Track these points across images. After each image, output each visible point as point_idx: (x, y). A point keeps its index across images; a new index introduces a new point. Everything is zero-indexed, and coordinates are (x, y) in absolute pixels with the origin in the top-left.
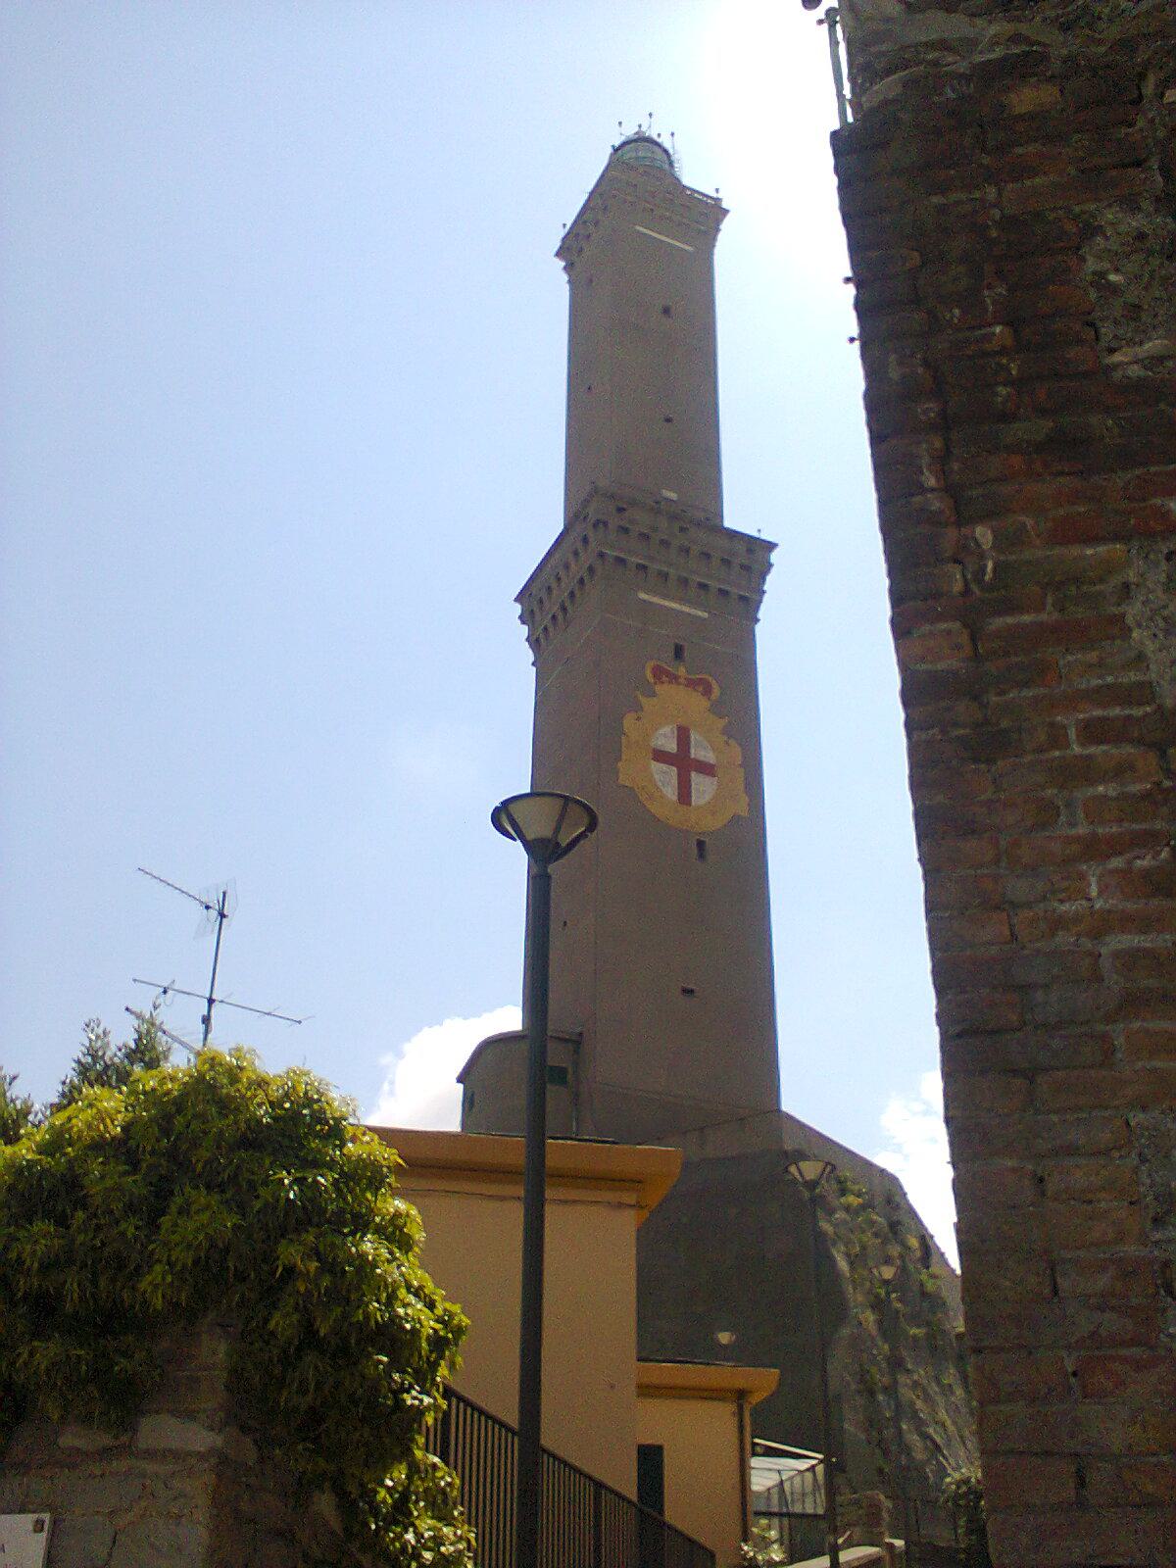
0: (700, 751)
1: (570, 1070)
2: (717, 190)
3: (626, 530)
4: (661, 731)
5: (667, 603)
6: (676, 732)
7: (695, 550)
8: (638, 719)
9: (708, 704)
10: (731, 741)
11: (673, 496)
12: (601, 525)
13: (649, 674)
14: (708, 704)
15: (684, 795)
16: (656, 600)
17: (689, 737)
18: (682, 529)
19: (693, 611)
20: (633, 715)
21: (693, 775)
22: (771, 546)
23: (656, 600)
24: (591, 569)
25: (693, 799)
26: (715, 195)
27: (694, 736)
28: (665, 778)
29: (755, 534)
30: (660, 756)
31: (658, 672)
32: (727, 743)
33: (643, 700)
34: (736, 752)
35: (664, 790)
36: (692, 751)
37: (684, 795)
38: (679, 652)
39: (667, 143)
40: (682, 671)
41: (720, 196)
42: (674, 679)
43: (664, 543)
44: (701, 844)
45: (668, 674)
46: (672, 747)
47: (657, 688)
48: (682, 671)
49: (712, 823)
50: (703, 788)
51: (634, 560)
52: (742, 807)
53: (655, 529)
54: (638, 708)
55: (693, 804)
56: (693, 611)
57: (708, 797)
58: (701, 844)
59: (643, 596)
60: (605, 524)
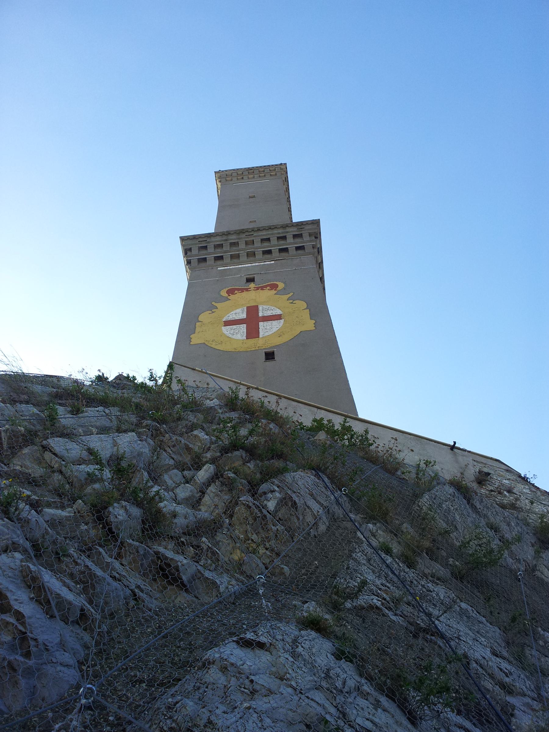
6: (245, 310)
12: (189, 253)
13: (224, 293)
21: (261, 324)
23: (231, 267)
34: (302, 305)
35: (234, 337)
40: (252, 285)
45: (238, 289)
53: (226, 240)
55: (260, 336)
57: (275, 330)
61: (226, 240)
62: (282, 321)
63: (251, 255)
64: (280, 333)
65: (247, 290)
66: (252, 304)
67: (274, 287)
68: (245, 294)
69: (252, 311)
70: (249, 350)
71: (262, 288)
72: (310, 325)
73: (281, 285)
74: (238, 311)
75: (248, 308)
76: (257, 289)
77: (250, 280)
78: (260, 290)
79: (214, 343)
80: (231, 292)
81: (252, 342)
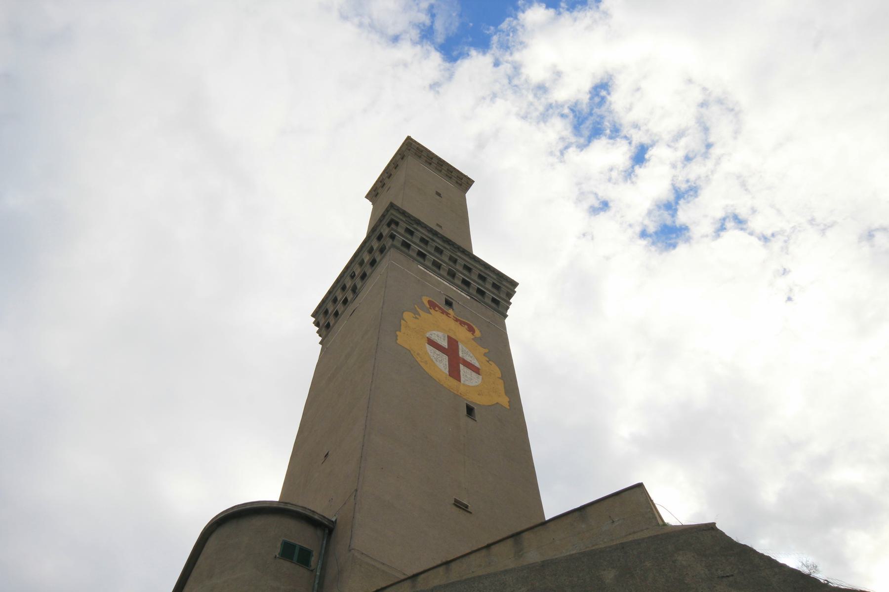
1: (315, 554)
9: (472, 337)
12: (393, 226)
14: (469, 335)
15: (454, 373)
17: (458, 346)
21: (461, 366)
25: (462, 379)
35: (437, 363)
37: (454, 373)
40: (450, 311)
44: (470, 411)
45: (440, 308)
46: (445, 344)
52: (504, 401)
60: (397, 224)
62: (480, 377)
63: (452, 274)
65: (447, 314)
66: (454, 337)
67: (471, 330)
68: (444, 316)
69: (453, 343)
71: (462, 323)
72: (504, 401)
73: (478, 333)
74: (440, 334)
75: (449, 337)
76: (457, 320)
77: (449, 303)
78: (458, 323)
80: (432, 305)
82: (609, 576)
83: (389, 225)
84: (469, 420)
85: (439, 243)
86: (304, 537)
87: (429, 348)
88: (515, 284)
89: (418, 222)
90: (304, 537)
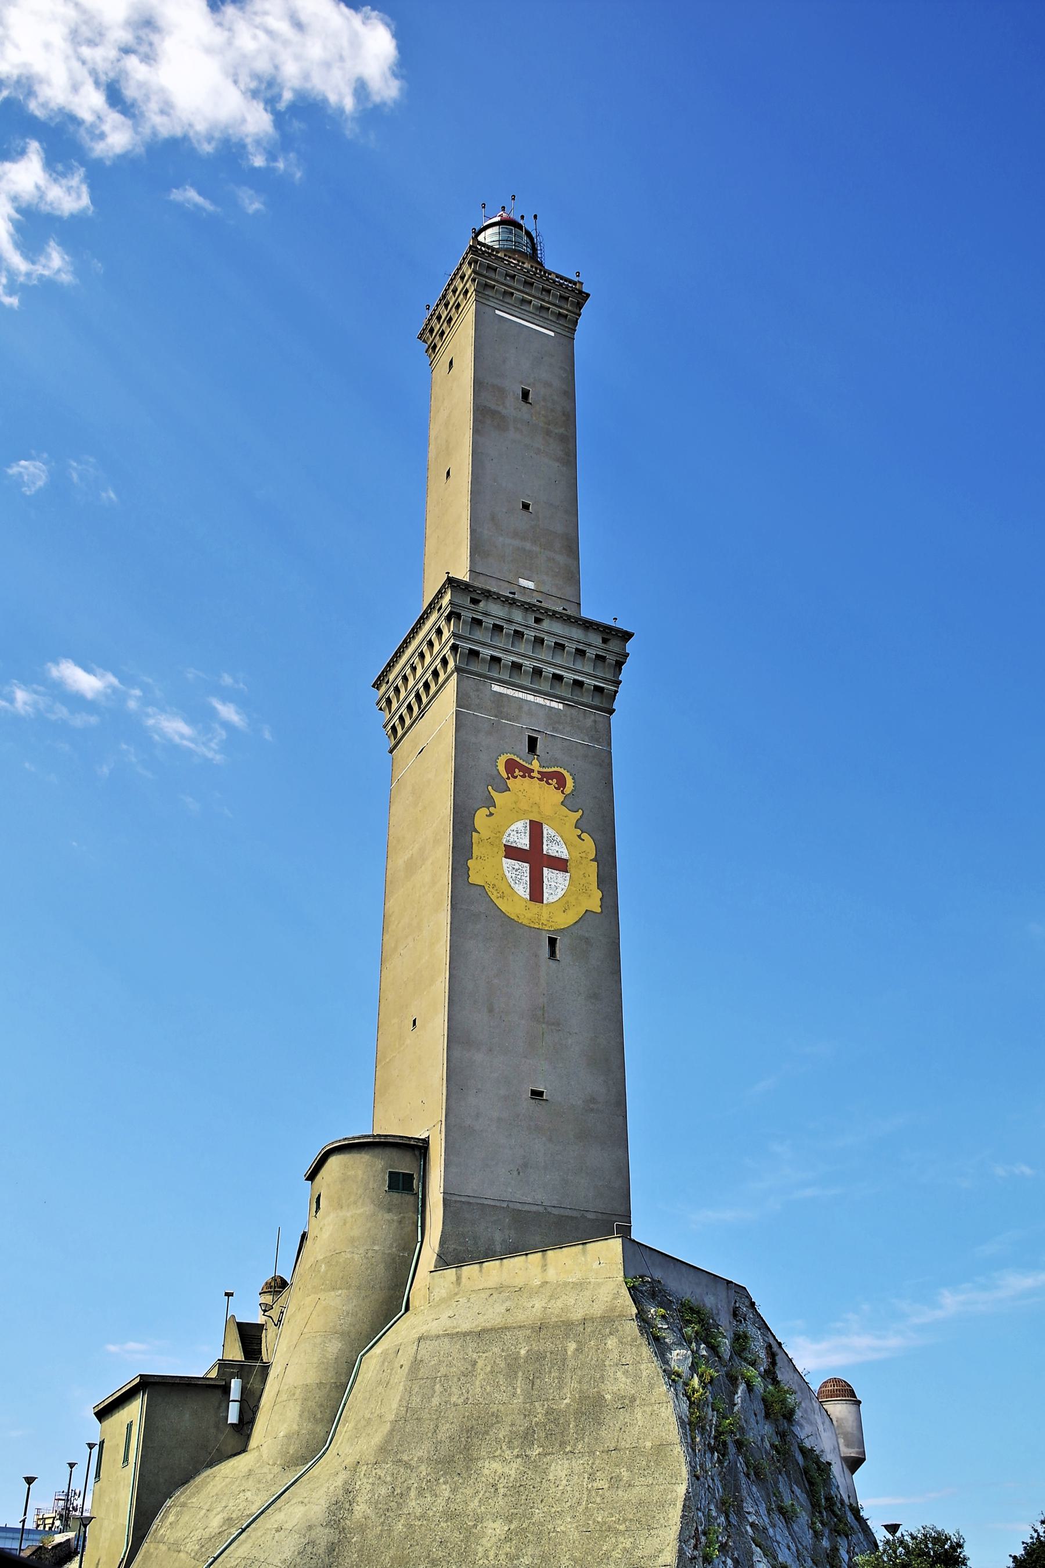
0: (553, 848)
2: (578, 275)
3: (478, 622)
4: (513, 827)
5: (520, 695)
7: (550, 641)
8: (491, 814)
9: (559, 797)
10: (584, 836)
11: (531, 585)
14: (559, 797)
15: (536, 893)
16: (510, 692)
18: (538, 621)
19: (548, 703)
20: (484, 811)
22: (627, 636)
23: (510, 692)
24: (445, 662)
25: (546, 895)
26: (576, 279)
27: (547, 831)
28: (517, 875)
29: (612, 623)
30: (512, 853)
31: (511, 766)
32: (579, 836)
33: (493, 793)
34: (588, 845)
35: (516, 887)
36: (545, 847)
37: (536, 893)
38: (532, 743)
39: (528, 224)
41: (580, 279)
42: (527, 772)
43: (518, 634)
44: (552, 942)
45: (522, 768)
46: (523, 842)
47: (511, 783)
48: (535, 765)
49: (564, 920)
50: (555, 883)
51: (486, 652)
53: (510, 621)
54: (490, 803)
55: (545, 902)
56: (548, 703)
57: (560, 894)
58: (552, 942)
59: (496, 688)
60: (459, 617)
61: (510, 621)
64: (565, 904)
67: (561, 784)
70: (532, 925)
72: (593, 901)
75: (532, 823)
79: (495, 893)
81: (535, 907)
82: (572, 1346)
83: (448, 619)
84: (551, 962)
85: (518, 616)
86: (405, 1165)
87: (508, 863)
88: (627, 636)
89: (488, 594)
90: (405, 1165)
